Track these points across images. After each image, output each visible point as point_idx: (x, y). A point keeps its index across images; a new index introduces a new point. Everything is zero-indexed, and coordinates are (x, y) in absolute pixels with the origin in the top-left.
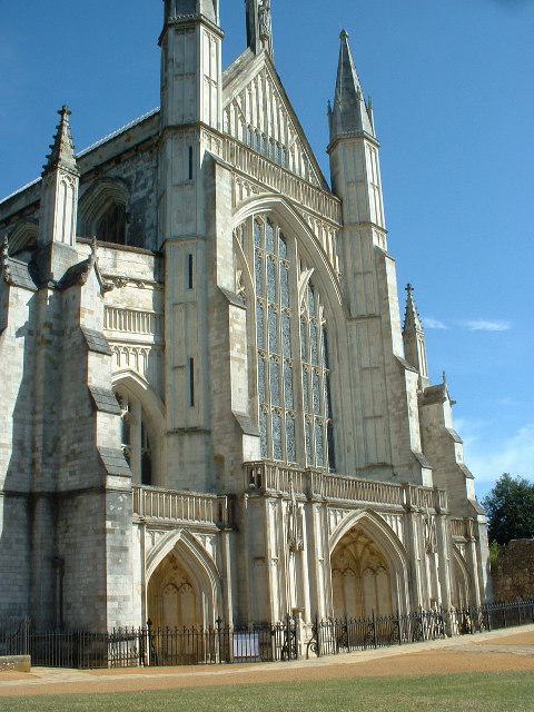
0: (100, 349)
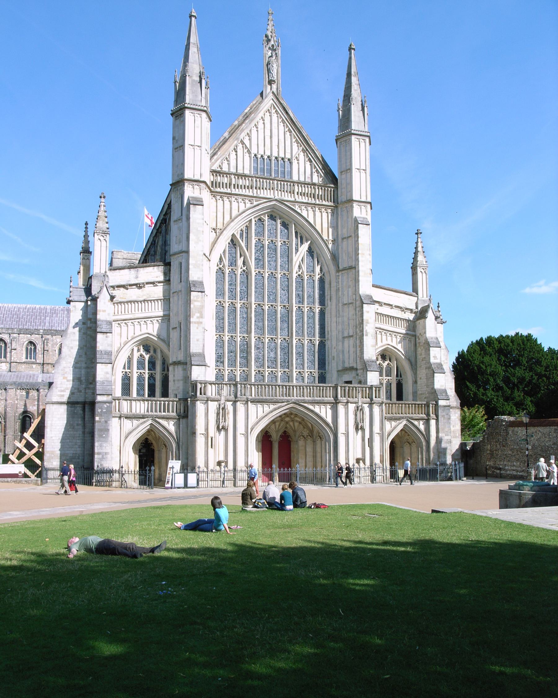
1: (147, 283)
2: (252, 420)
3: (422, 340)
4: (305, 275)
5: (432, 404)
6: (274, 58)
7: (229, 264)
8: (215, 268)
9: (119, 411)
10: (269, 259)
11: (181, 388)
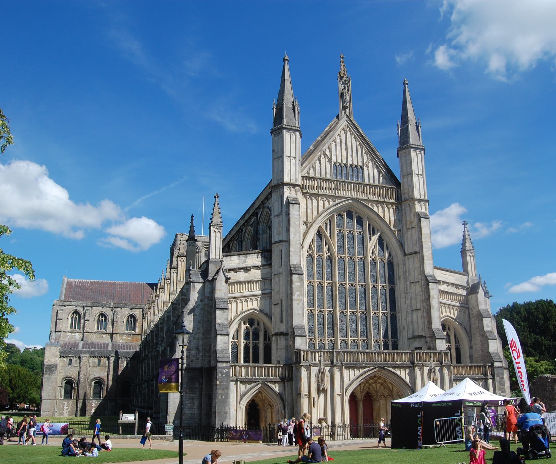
0: (223, 307)
1: (254, 267)
2: (347, 382)
3: (475, 312)
4: (378, 259)
5: (489, 366)
6: (347, 89)
7: (316, 250)
8: (306, 254)
9: (235, 375)
10: (349, 246)
11: (284, 356)
